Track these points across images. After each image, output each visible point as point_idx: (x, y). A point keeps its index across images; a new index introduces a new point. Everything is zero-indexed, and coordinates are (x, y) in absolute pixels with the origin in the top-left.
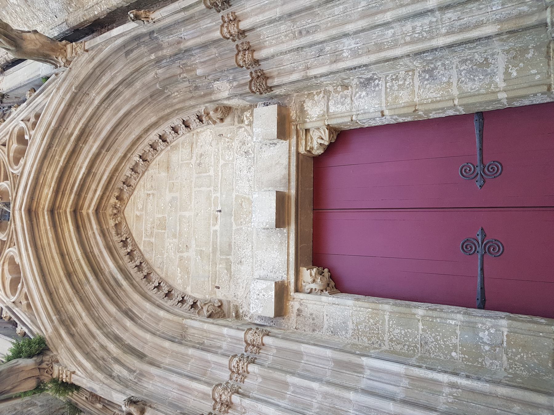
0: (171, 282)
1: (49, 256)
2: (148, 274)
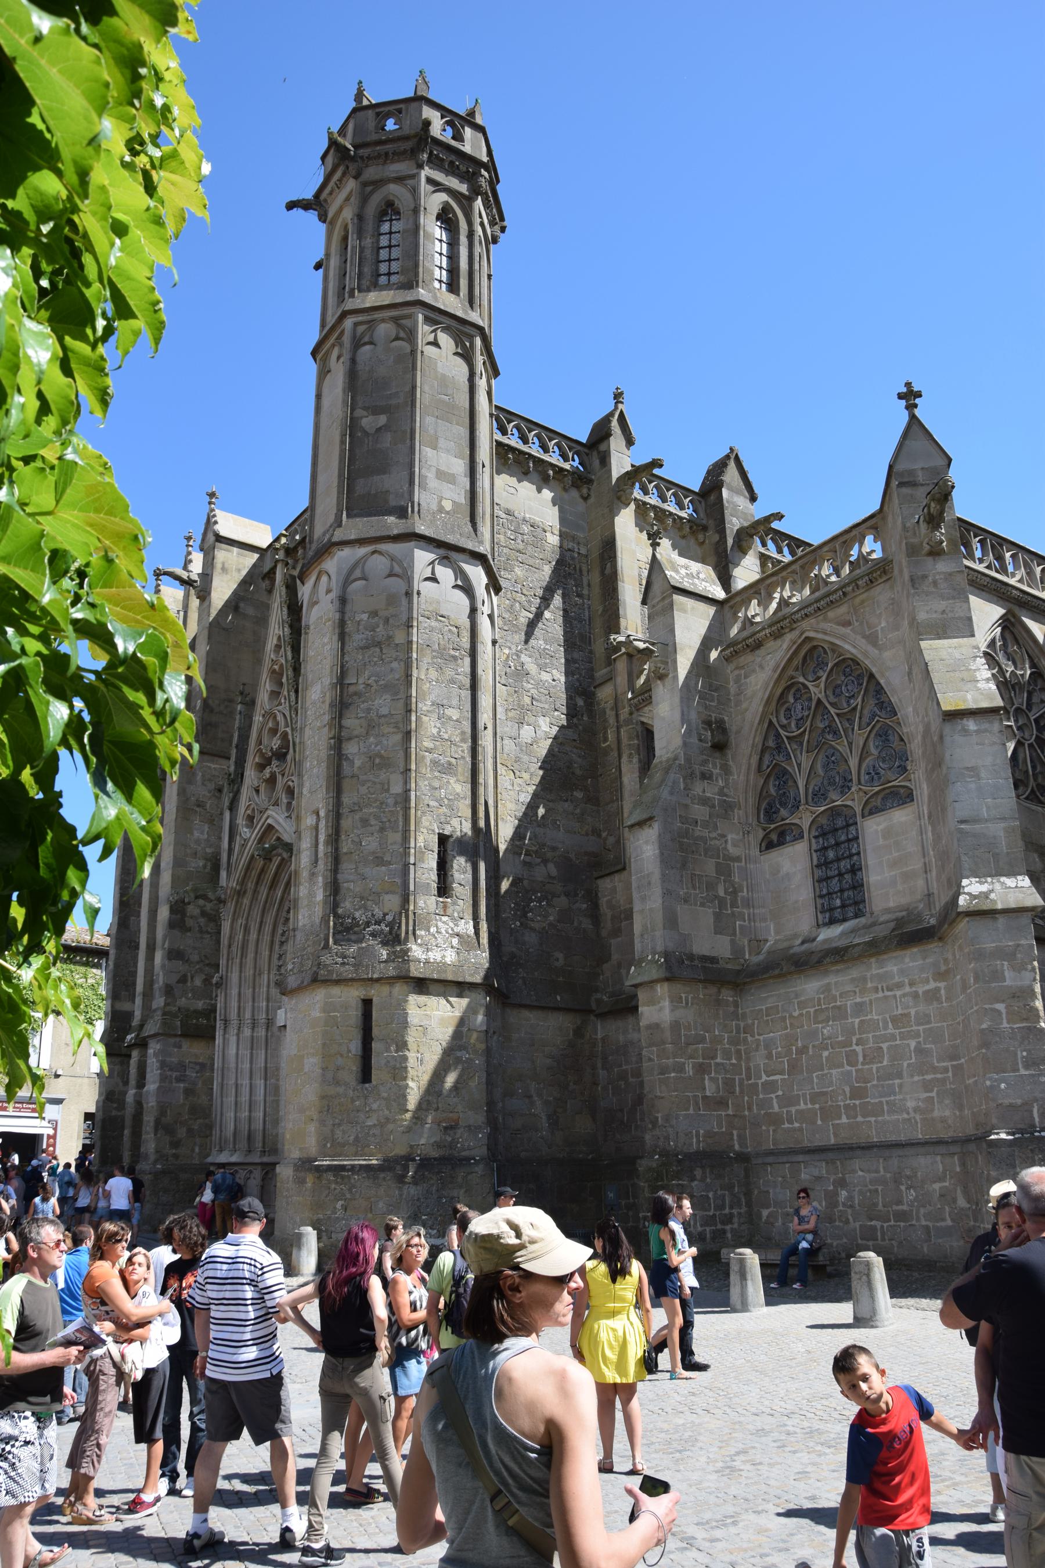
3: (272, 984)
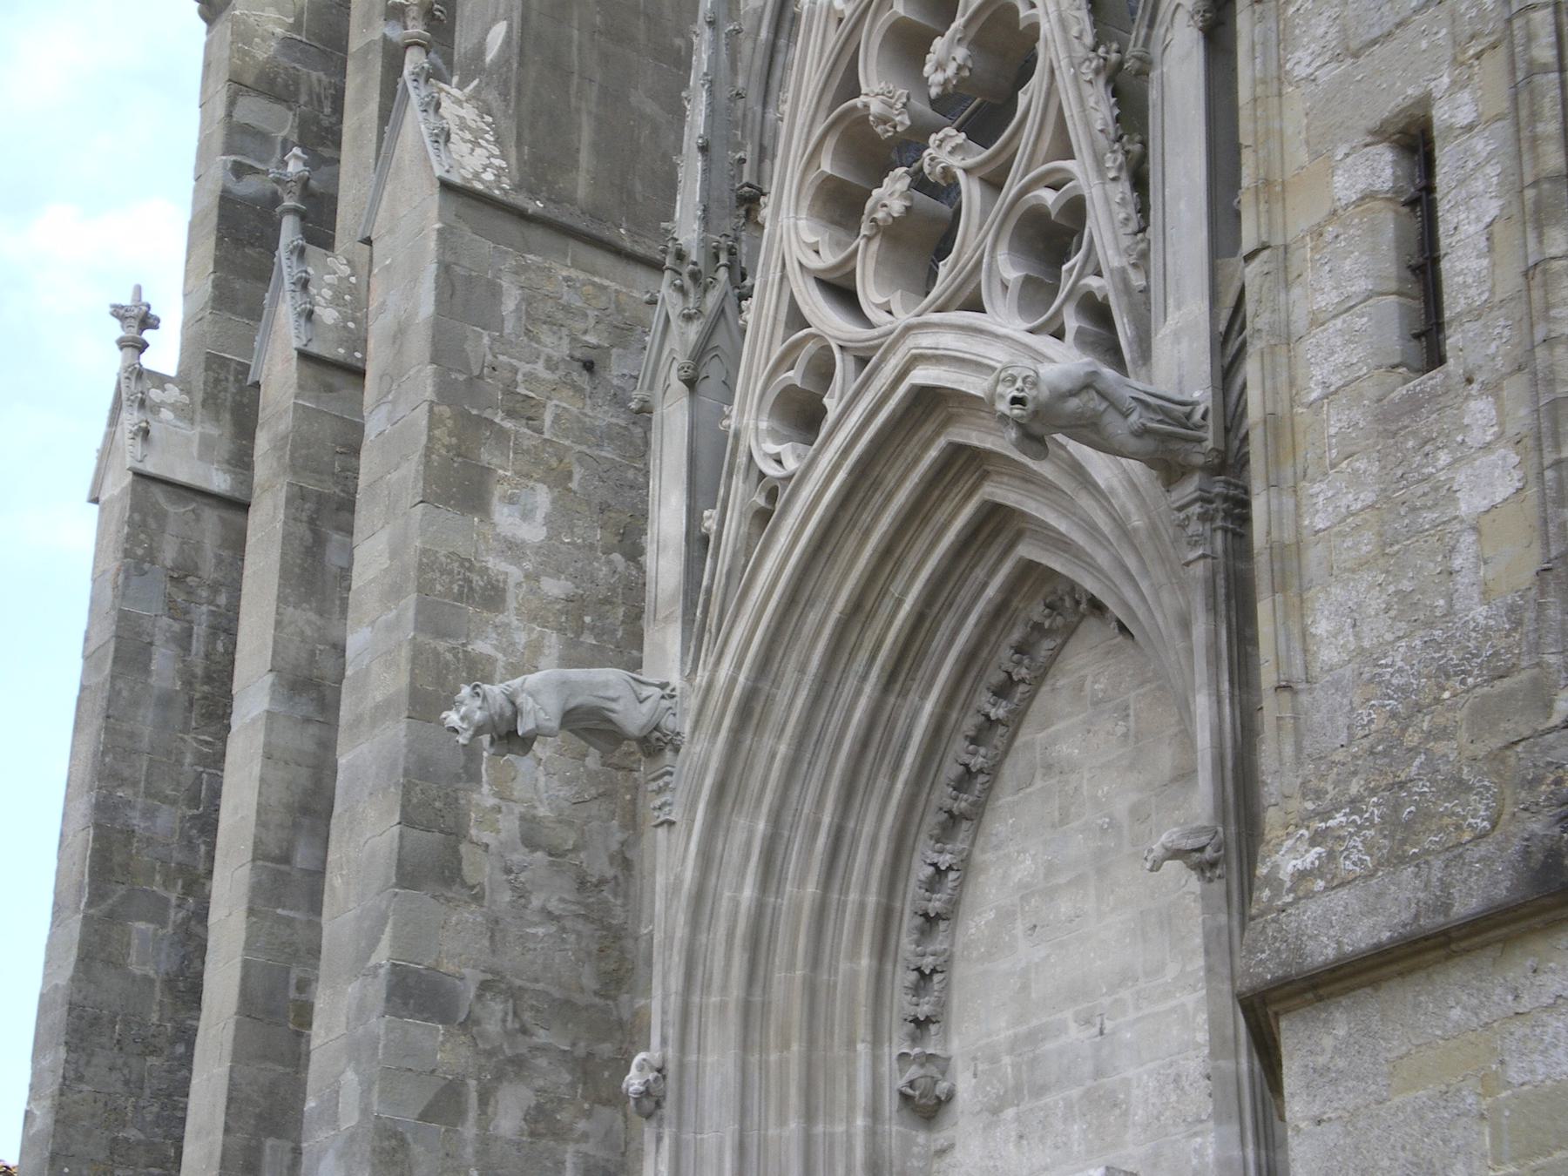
0: (967, 900)
1: (866, 517)
2: (964, 816)
3: (890, 1103)
